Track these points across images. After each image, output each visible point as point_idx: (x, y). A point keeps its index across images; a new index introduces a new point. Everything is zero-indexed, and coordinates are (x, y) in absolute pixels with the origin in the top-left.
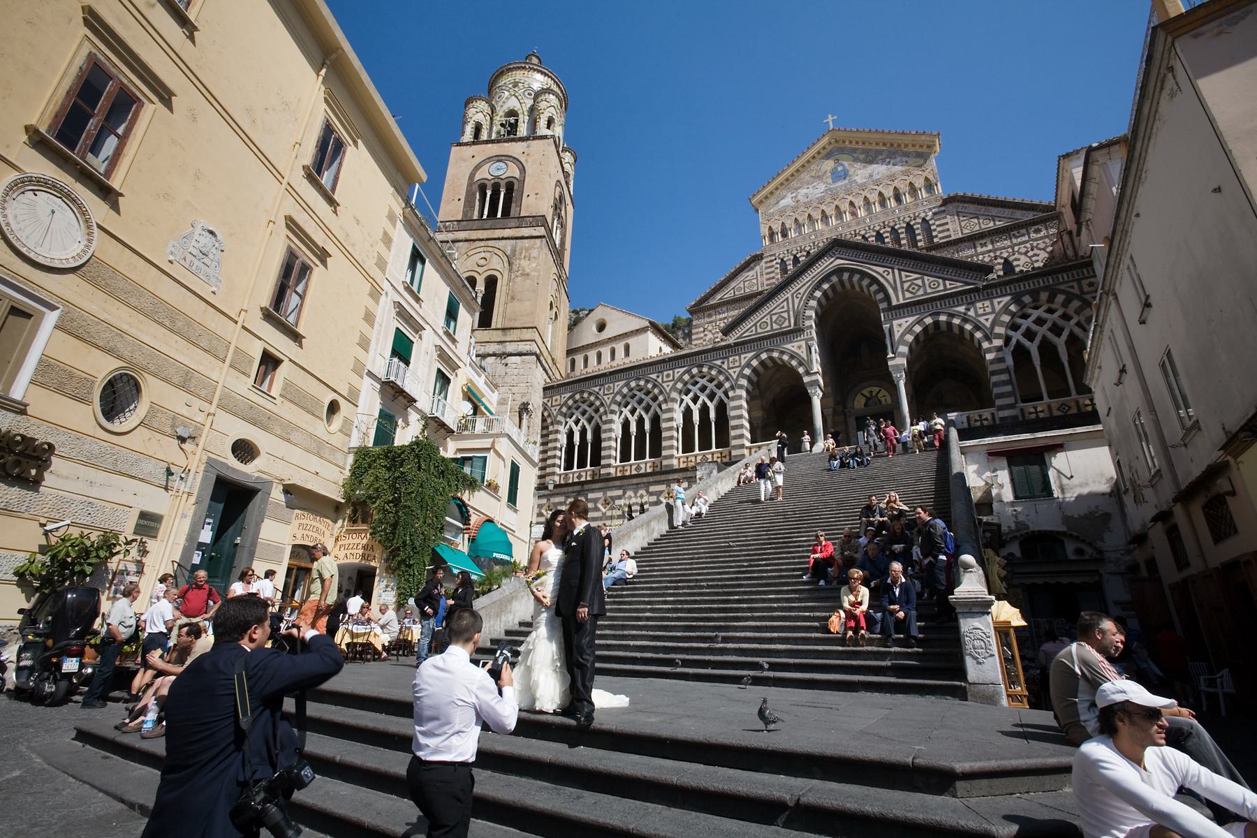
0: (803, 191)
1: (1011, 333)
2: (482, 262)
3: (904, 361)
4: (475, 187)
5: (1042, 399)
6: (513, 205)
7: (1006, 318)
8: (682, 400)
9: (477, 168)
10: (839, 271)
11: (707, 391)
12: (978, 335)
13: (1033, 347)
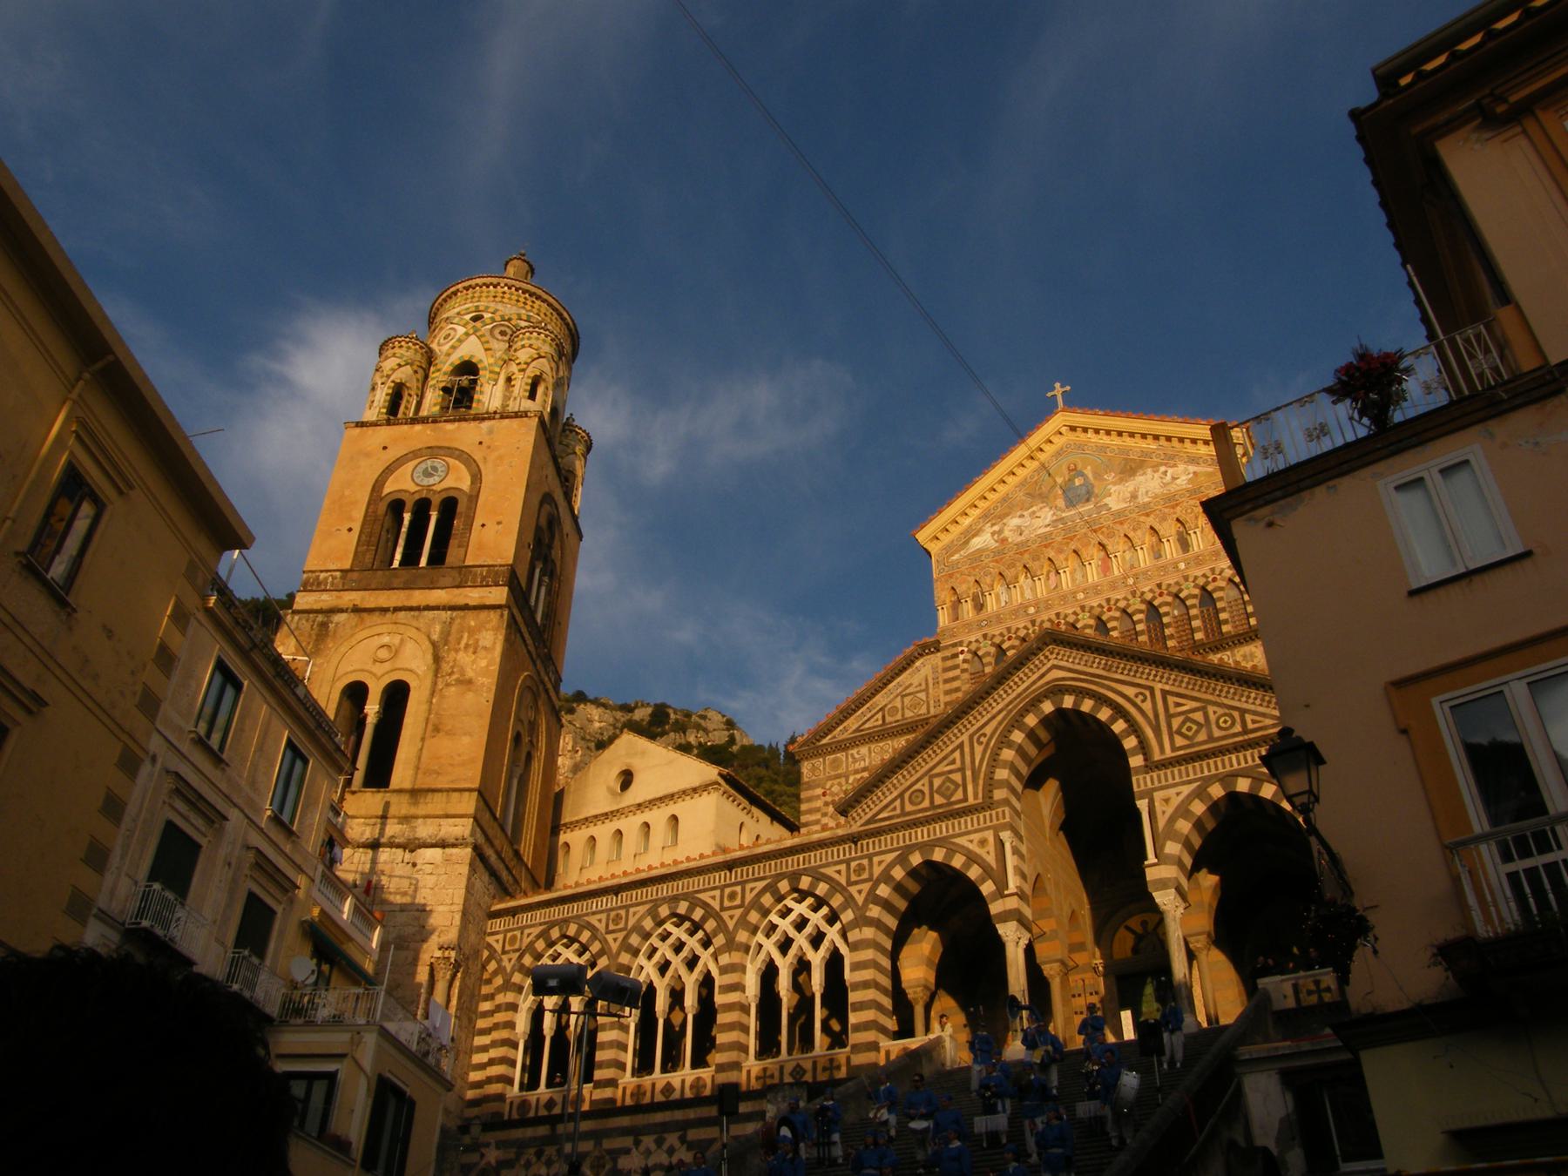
0: (1014, 522)
2: (383, 654)
3: (1169, 872)
4: (382, 507)
6: (453, 542)
8: (761, 946)
9: (389, 470)
10: (1056, 690)
11: (809, 929)
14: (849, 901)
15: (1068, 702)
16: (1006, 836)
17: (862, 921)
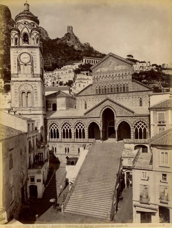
0: (103, 69)
1: (136, 126)
3: (117, 128)
5: (138, 139)
7: (135, 123)
12: (130, 125)
13: (138, 129)
14: (85, 125)
15: (109, 107)
16: (101, 120)
17: (87, 127)
